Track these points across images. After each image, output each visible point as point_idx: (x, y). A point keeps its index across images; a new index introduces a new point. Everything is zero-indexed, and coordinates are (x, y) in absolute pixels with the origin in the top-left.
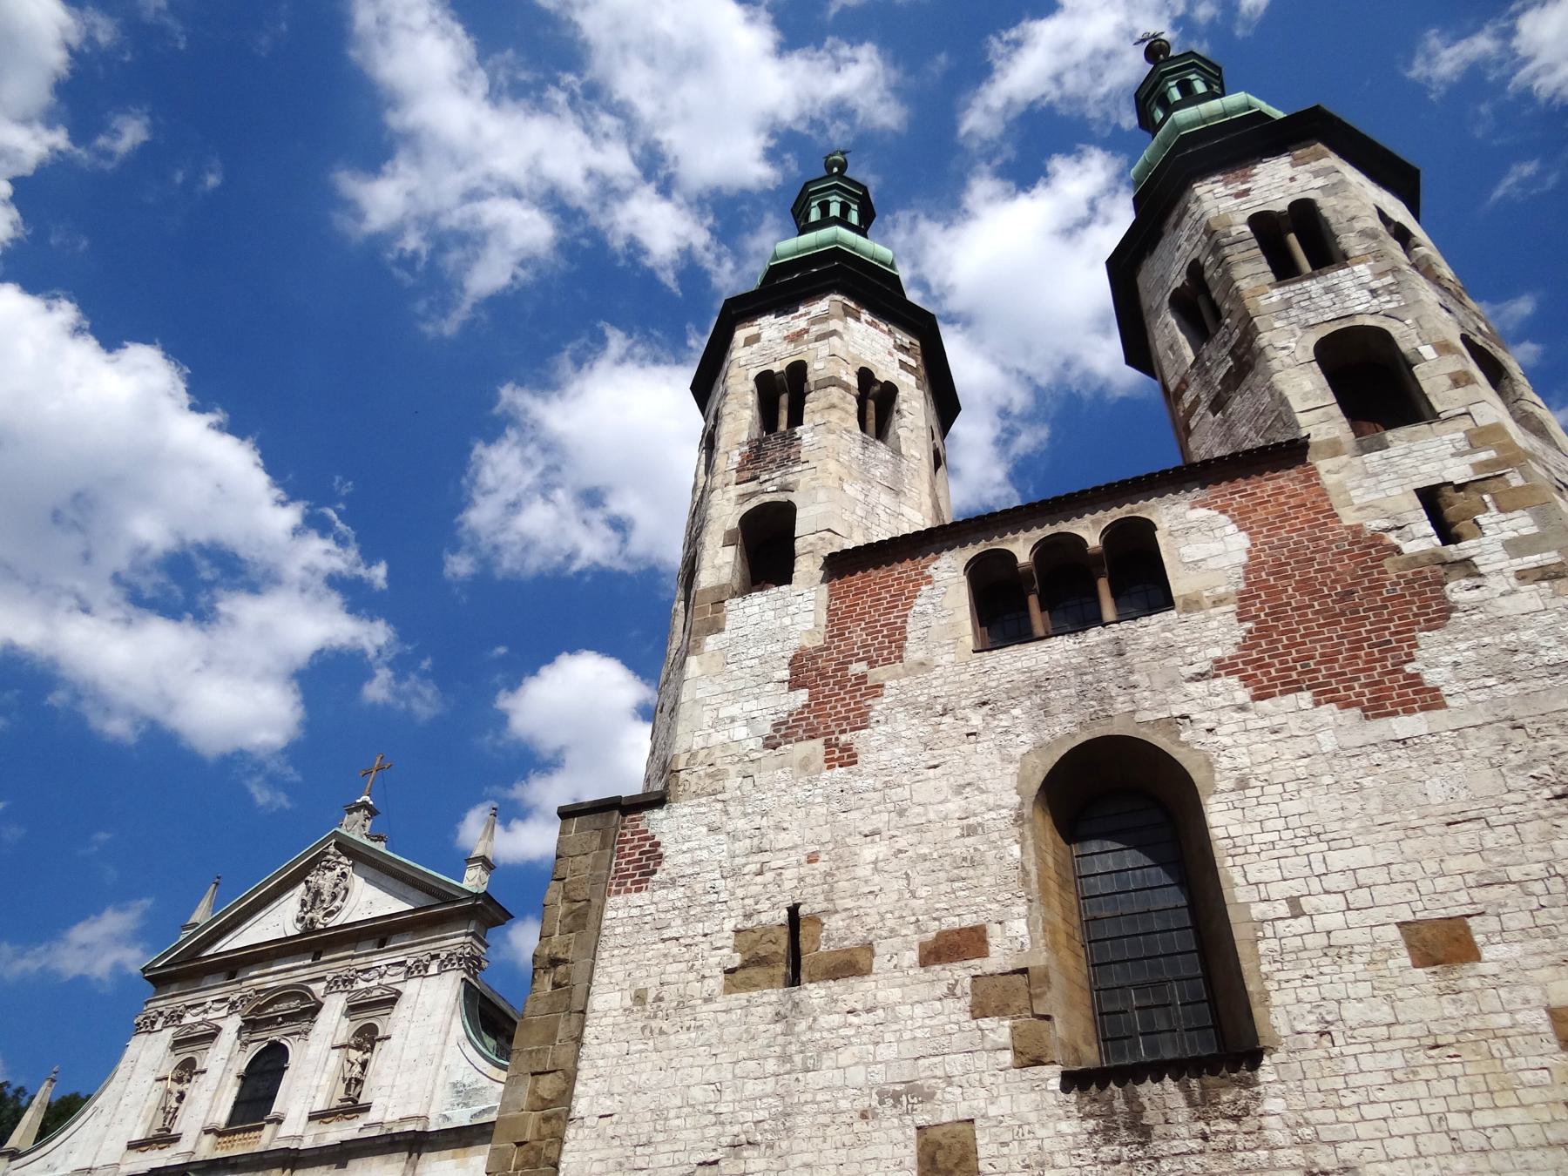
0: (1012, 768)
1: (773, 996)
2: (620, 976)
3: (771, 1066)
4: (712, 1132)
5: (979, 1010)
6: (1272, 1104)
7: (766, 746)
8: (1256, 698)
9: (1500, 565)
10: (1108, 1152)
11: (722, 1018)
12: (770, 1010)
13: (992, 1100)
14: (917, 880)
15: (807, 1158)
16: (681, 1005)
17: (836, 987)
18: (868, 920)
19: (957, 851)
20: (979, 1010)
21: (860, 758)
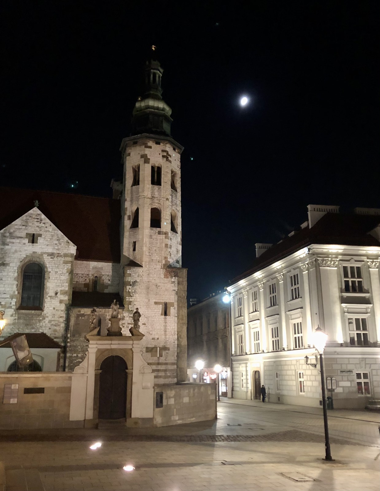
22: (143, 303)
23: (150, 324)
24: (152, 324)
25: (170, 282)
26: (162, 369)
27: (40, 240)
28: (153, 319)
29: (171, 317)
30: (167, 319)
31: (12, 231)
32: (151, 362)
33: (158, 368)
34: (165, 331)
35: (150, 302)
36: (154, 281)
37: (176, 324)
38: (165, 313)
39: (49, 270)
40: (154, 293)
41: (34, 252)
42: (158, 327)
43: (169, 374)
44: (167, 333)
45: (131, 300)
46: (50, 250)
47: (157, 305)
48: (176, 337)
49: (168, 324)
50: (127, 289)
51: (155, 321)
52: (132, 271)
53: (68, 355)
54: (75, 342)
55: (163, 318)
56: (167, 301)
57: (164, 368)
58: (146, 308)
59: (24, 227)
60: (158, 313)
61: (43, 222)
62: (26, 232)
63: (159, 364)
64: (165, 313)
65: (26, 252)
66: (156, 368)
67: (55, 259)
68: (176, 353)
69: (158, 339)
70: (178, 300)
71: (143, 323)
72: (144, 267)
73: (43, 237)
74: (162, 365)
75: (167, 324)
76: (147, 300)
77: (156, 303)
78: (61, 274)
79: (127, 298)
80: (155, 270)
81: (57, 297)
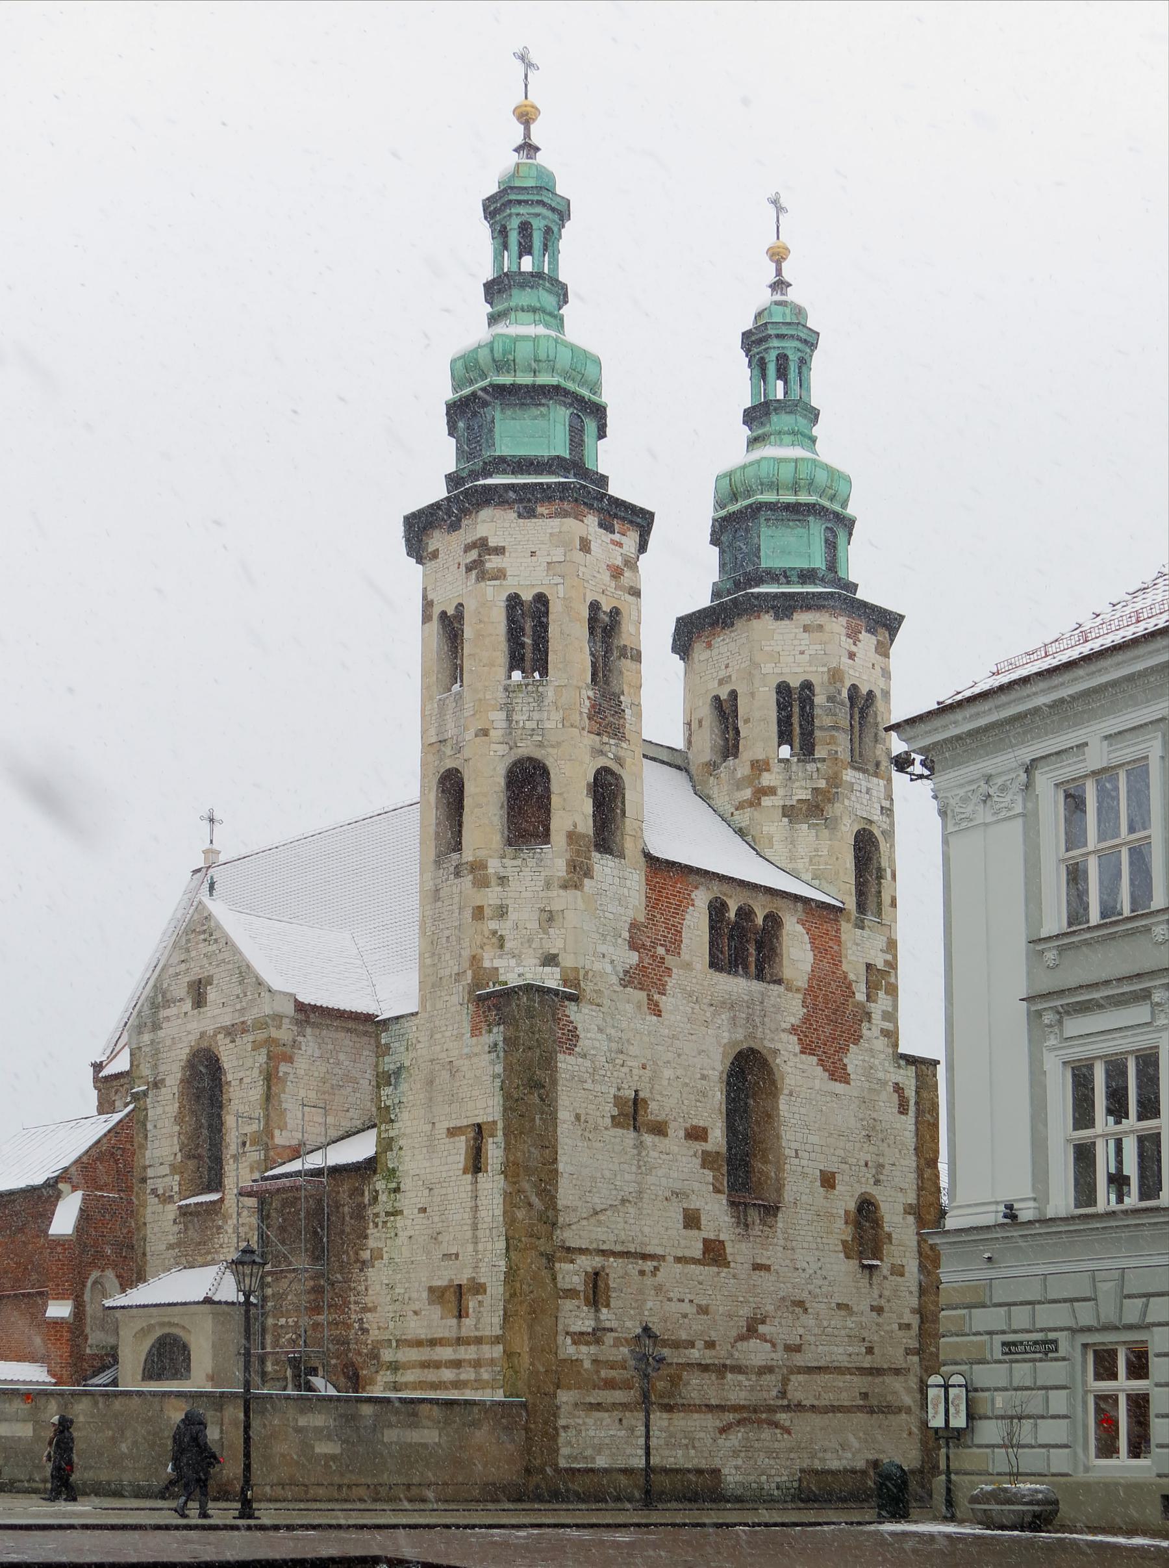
0: (721, 1050)
1: (632, 1134)
2: (567, 1103)
3: (634, 1169)
4: (614, 1192)
5: (703, 1166)
6: (780, 1225)
8: (802, 1052)
9: (879, 1022)
10: (738, 1231)
11: (613, 1140)
12: (632, 1143)
13: (706, 1204)
14: (684, 1095)
15: (649, 1212)
16: (596, 1129)
17: (657, 1139)
18: (666, 1109)
19: (699, 1086)
20: (703, 1166)
21: (663, 1014)
25: (487, 1049)
29: (491, 1174)
34: (475, 1227)
38: (476, 1164)
40: (446, 1098)
42: (456, 1217)
44: (480, 1233)
48: (502, 1245)
49: (483, 1201)
51: (450, 1197)
55: (469, 1182)
56: (479, 1120)
57: (475, 1357)
60: (455, 1166)
68: (502, 1303)
74: (469, 1344)
75: (479, 1203)
77: (452, 1132)
80: (447, 1016)
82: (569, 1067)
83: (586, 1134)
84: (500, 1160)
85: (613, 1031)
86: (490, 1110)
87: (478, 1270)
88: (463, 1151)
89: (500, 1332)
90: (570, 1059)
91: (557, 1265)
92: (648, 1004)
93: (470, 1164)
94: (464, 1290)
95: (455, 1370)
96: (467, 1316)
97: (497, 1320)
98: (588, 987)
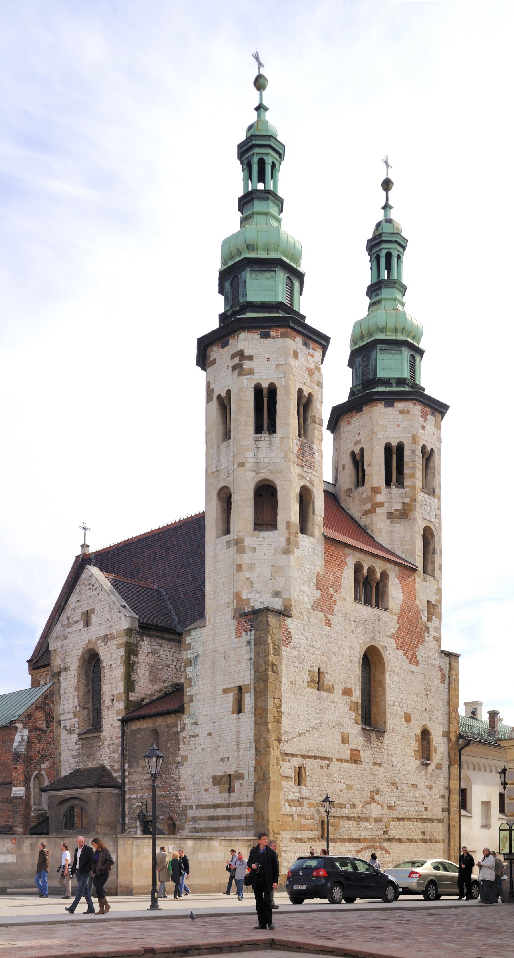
7: (312, 609)
22: (208, 695)
23: (217, 733)
24: (220, 733)
26: (234, 814)
27: (94, 619)
28: (221, 723)
29: (246, 713)
30: (240, 720)
31: (69, 615)
32: (220, 802)
33: (230, 814)
34: (238, 744)
35: (217, 691)
36: (221, 648)
37: (253, 728)
39: (104, 664)
41: (90, 641)
43: (244, 824)
44: (241, 746)
45: (192, 693)
46: (103, 633)
47: (225, 695)
48: (253, 752)
50: (187, 673)
52: (193, 637)
53: (127, 796)
54: (134, 777)
58: (212, 705)
59: (79, 603)
61: (94, 587)
62: (81, 611)
63: (230, 805)
64: (239, 709)
65: (83, 643)
66: (226, 814)
67: (109, 643)
68: (253, 784)
69: (228, 759)
70: (255, 677)
71: (208, 732)
72: (207, 624)
73: (96, 612)
74: (234, 807)
76: (211, 689)
77: (225, 691)
78: (115, 668)
79: (188, 690)
81: (113, 706)
82: (287, 654)
83: (295, 691)
84: (252, 705)
85: (308, 634)
86: (246, 678)
87: (239, 766)
88: (231, 701)
89: (252, 800)
90: (288, 649)
91: (282, 763)
92: (326, 620)
93: (236, 708)
94: (232, 777)
95: (227, 821)
96: (234, 791)
97: (251, 793)
98: (294, 611)
